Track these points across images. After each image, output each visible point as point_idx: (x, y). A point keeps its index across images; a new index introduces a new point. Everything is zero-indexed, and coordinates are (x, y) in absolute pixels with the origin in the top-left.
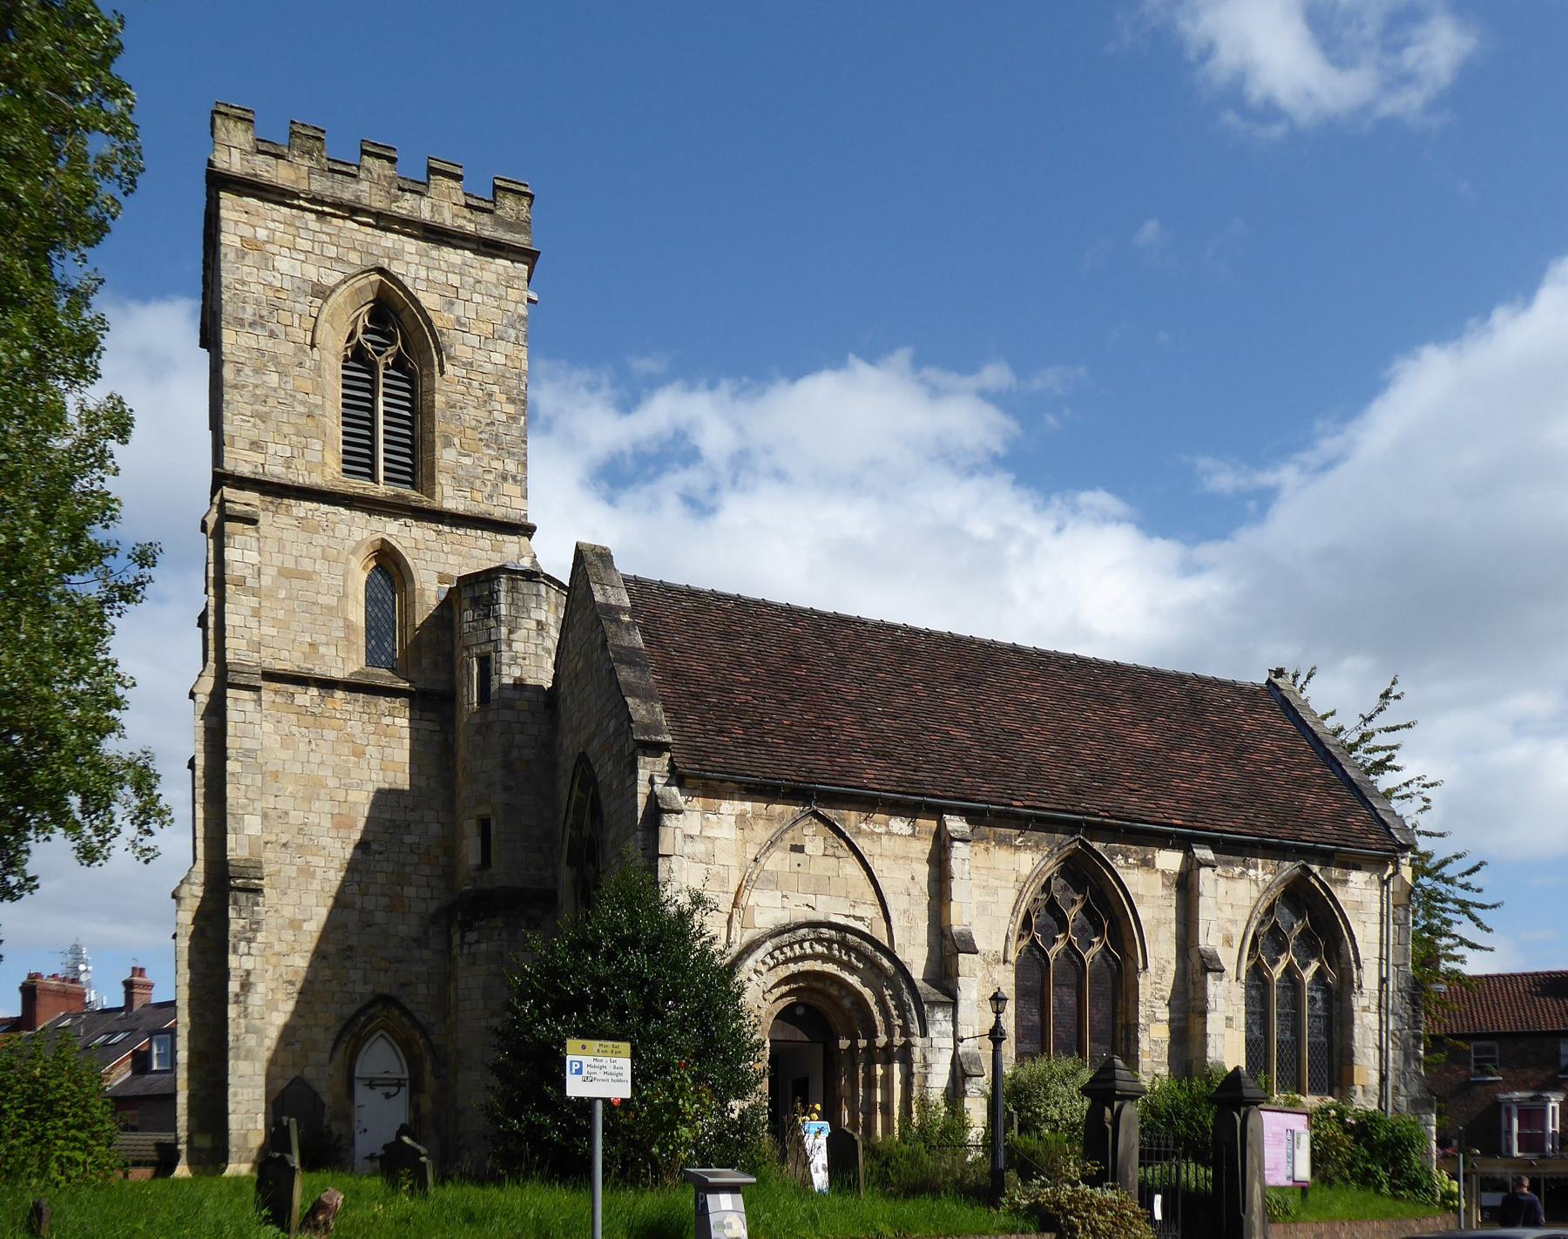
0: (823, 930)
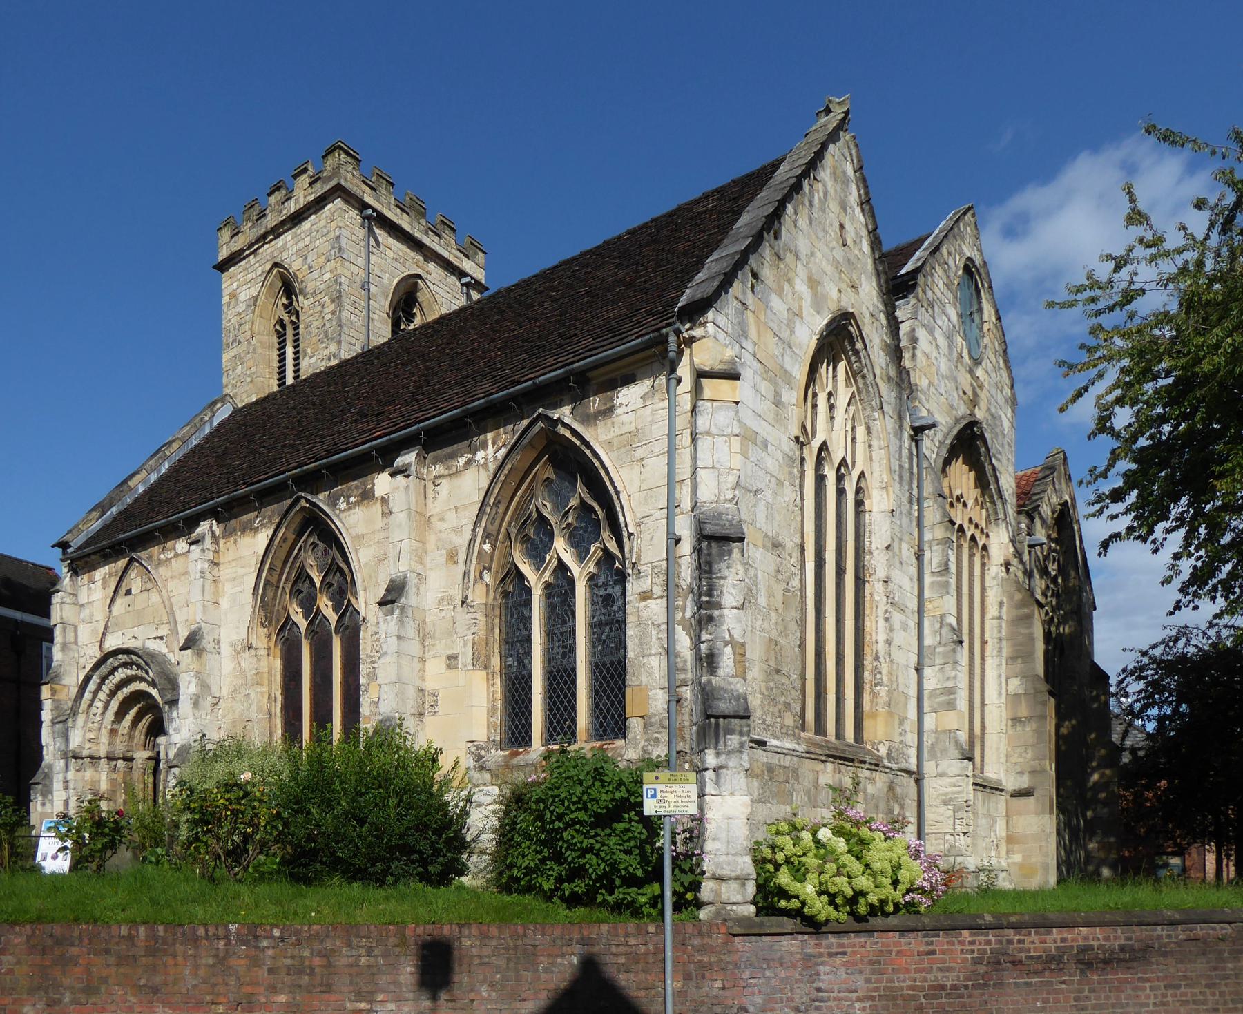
0: (120, 656)
